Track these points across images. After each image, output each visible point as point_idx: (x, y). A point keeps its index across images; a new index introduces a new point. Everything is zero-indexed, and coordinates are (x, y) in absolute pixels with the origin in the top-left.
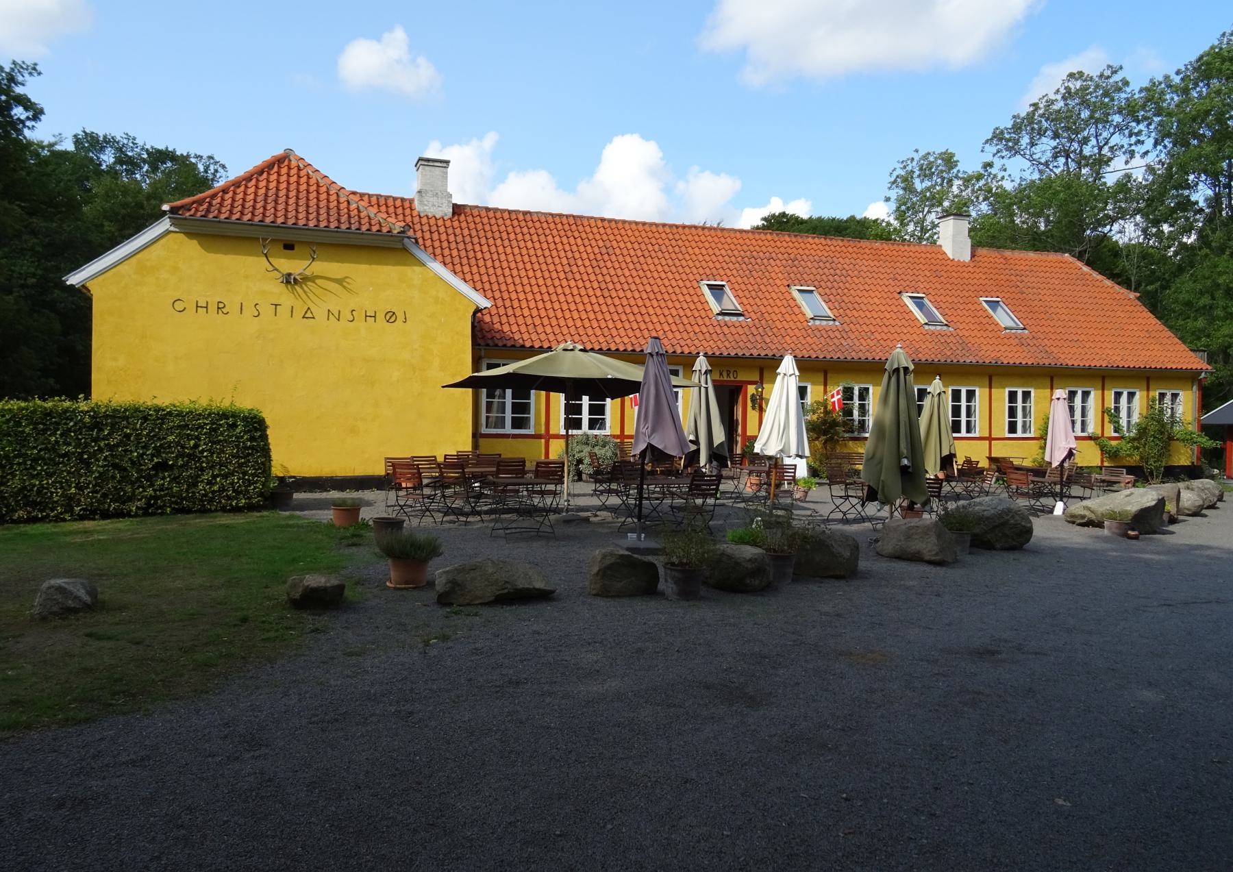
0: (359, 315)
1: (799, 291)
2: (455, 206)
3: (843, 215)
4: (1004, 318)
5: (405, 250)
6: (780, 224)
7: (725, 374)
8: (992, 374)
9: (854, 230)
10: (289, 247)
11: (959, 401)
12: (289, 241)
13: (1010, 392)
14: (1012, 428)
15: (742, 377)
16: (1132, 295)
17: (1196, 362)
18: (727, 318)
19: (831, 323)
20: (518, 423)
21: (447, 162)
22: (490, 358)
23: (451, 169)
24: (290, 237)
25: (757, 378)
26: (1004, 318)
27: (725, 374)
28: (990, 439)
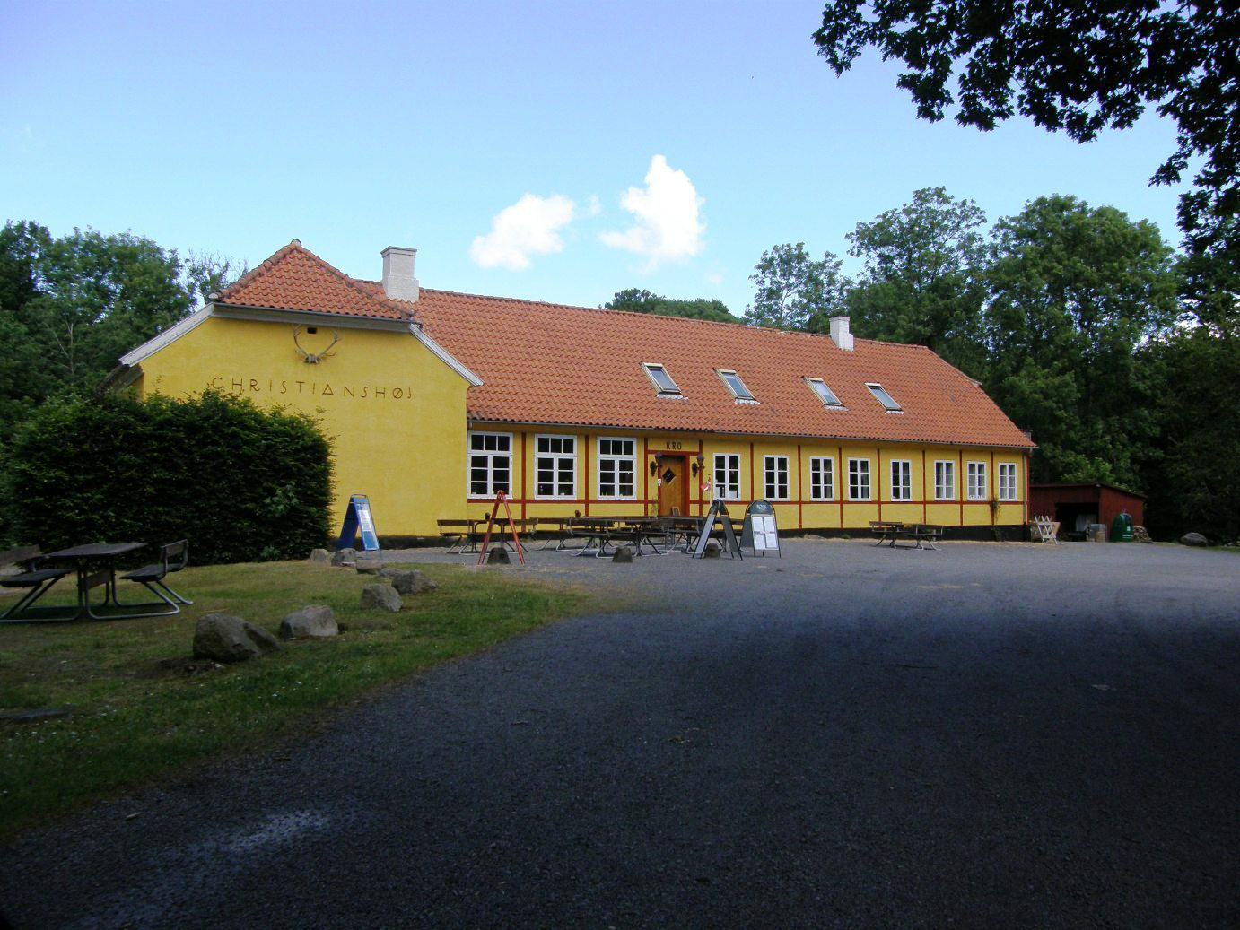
0: (371, 393)
1: (651, 368)
2: (421, 290)
3: (692, 298)
4: (821, 391)
5: (411, 333)
6: (629, 303)
7: (671, 446)
8: (880, 446)
9: (713, 312)
10: (312, 331)
11: (856, 470)
12: (313, 323)
13: (937, 464)
14: (816, 493)
15: (685, 448)
16: (976, 384)
17: (1023, 439)
18: (668, 396)
19: (752, 402)
20: (563, 489)
21: (415, 251)
22: (541, 433)
23: (417, 258)
24: (313, 323)
25: (697, 450)
26: (821, 391)
27: (671, 446)
28: (880, 503)
